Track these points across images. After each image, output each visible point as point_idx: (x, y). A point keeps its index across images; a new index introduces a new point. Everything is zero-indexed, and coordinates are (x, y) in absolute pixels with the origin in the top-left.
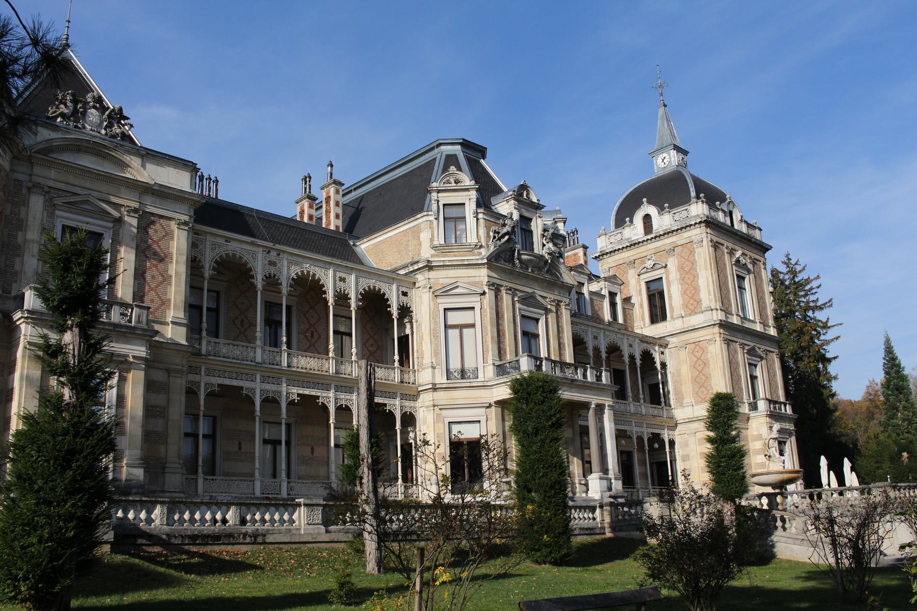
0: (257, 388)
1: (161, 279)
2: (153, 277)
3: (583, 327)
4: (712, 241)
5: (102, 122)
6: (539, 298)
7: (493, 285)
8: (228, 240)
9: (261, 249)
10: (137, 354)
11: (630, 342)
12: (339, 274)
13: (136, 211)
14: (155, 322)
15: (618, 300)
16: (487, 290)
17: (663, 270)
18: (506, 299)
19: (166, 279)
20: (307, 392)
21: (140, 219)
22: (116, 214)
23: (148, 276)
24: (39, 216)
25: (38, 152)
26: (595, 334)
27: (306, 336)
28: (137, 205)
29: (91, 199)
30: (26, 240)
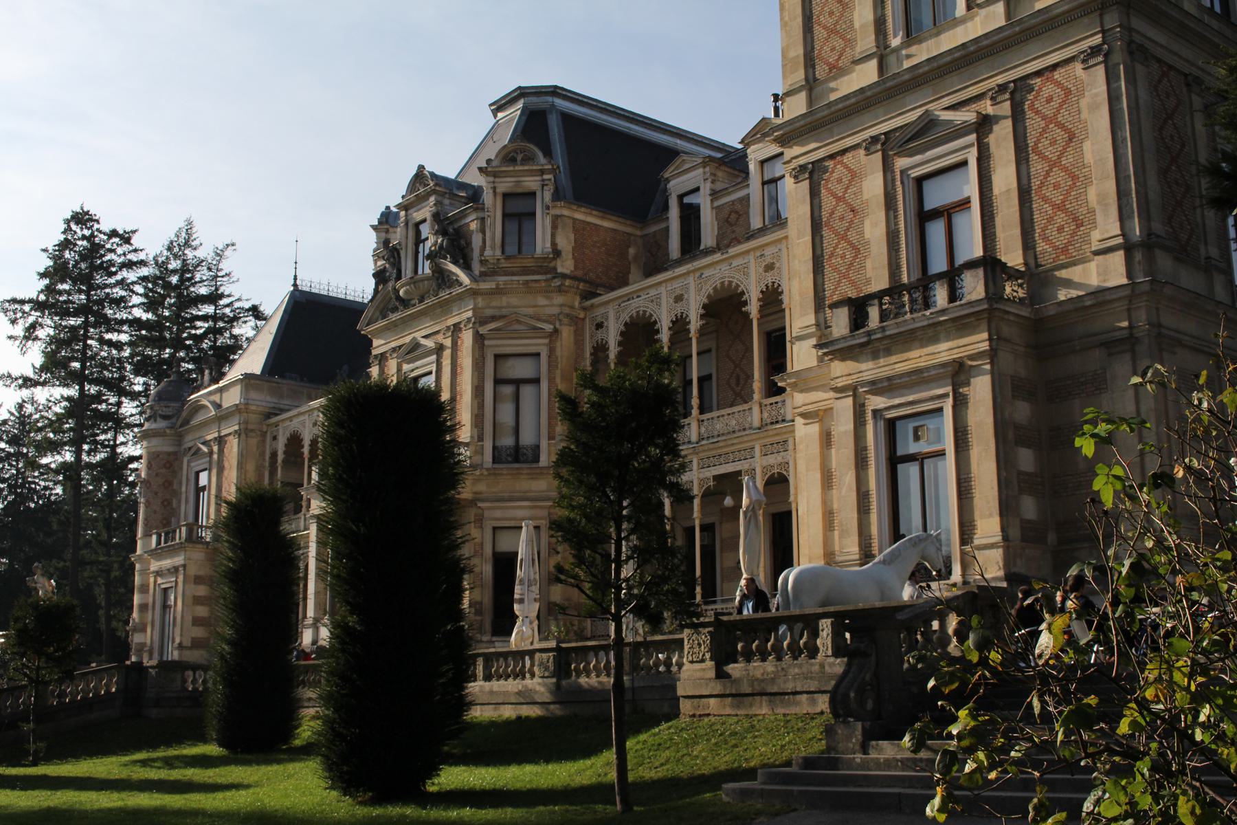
3: (653, 292)
8: (290, 419)
11: (768, 260)
26: (678, 292)
28: (216, 435)
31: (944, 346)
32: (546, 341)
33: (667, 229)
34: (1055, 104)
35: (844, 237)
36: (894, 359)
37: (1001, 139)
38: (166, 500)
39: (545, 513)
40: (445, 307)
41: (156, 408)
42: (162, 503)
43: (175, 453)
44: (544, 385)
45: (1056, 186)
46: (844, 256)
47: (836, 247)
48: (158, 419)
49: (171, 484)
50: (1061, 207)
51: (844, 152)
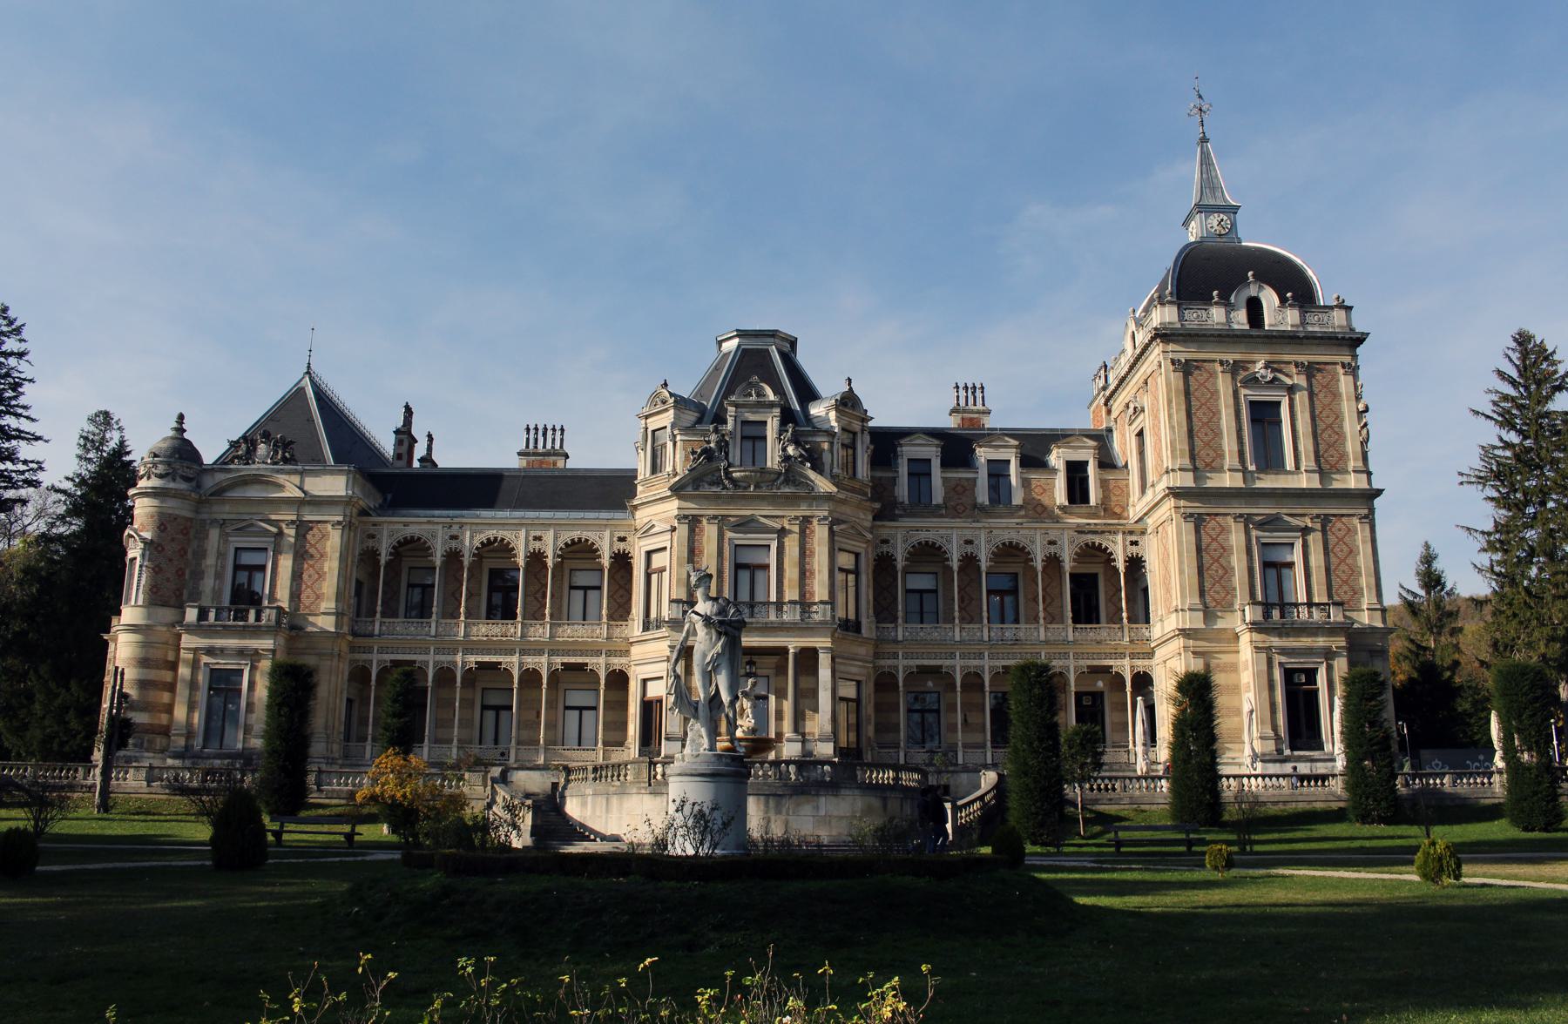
0: (430, 661)
1: (316, 576)
2: (310, 576)
3: (942, 532)
4: (1173, 362)
5: (269, 453)
6: (763, 520)
7: (686, 517)
8: (406, 524)
9: (440, 527)
10: (266, 647)
11: (1052, 538)
12: (533, 534)
13: (293, 522)
14: (309, 615)
15: (1091, 470)
16: (676, 525)
17: (1142, 415)
18: (710, 532)
19: (321, 576)
20: (486, 658)
21: (297, 529)
22: (274, 530)
23: (305, 576)
24: (216, 545)
25: (211, 495)
27: (536, 598)
28: (294, 518)
29: (254, 522)
30: (207, 566)
31: (1321, 639)
32: (864, 545)
33: (894, 479)
34: (1343, 533)
35: (1217, 561)
36: (1291, 639)
37: (1315, 539)
38: (180, 569)
39: (864, 671)
40: (792, 501)
41: (177, 466)
42: (177, 571)
43: (190, 520)
44: (864, 578)
45: (1344, 571)
46: (1217, 571)
47: (1212, 564)
48: (178, 479)
49: (186, 553)
50: (1346, 582)
51: (1217, 515)
